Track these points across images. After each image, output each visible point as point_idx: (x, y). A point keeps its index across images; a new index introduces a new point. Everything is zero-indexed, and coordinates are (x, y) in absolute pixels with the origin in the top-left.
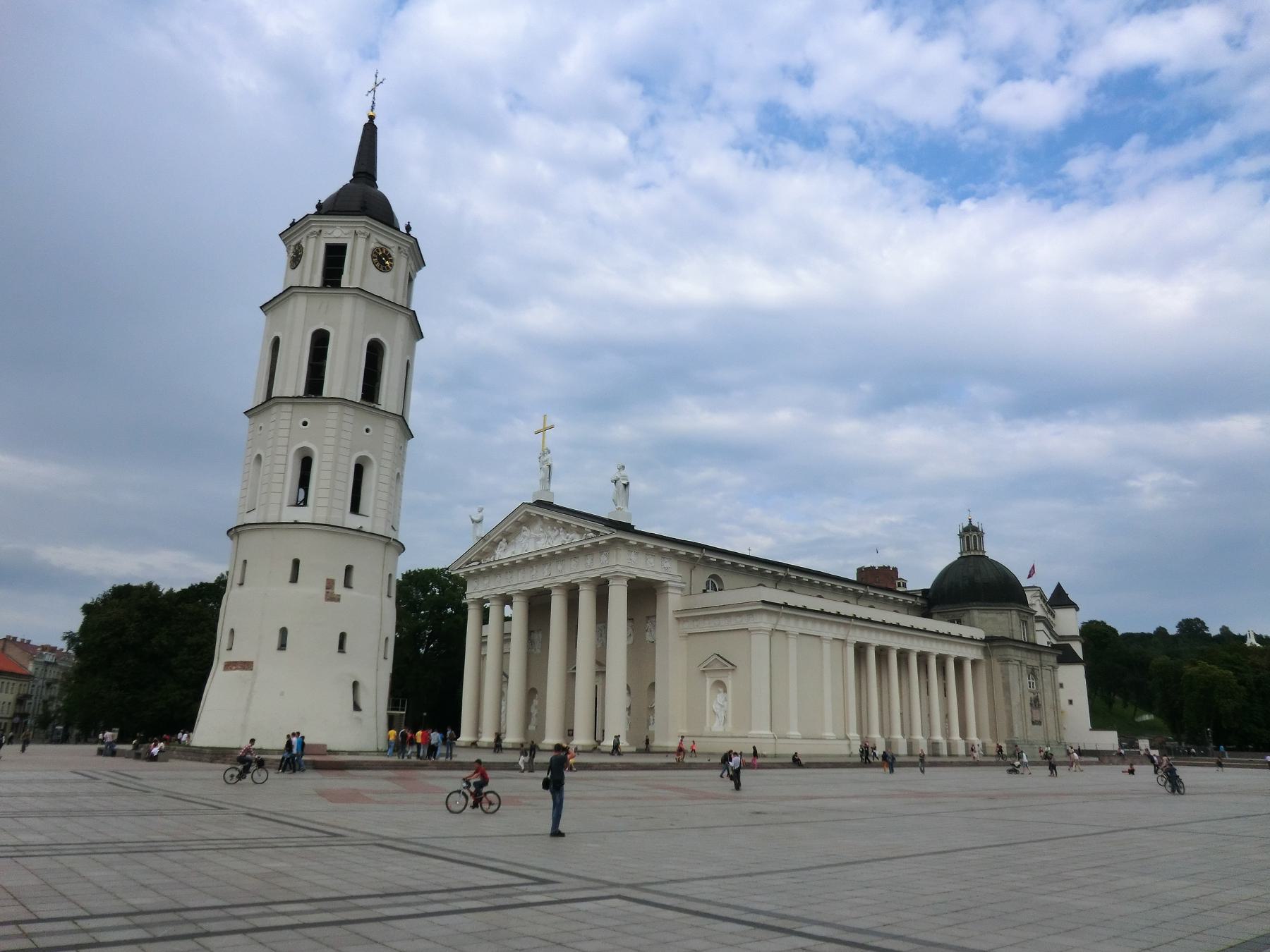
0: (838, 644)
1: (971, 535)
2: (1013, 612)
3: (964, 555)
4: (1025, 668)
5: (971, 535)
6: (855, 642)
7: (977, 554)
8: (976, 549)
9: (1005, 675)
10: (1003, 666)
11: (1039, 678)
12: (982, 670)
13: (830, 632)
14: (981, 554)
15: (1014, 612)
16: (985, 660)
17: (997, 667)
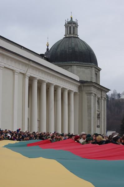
0: (21, 76)
1: (71, 26)
2: (93, 68)
3: (67, 36)
4: (96, 98)
5: (71, 26)
6: (29, 76)
7: (74, 36)
8: (74, 33)
9: (89, 101)
10: (88, 96)
11: (100, 103)
12: (78, 97)
13: (19, 68)
14: (77, 36)
15: (93, 68)
16: (79, 93)
17: (85, 96)
